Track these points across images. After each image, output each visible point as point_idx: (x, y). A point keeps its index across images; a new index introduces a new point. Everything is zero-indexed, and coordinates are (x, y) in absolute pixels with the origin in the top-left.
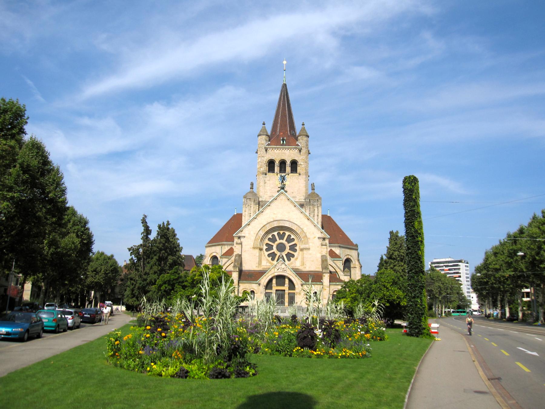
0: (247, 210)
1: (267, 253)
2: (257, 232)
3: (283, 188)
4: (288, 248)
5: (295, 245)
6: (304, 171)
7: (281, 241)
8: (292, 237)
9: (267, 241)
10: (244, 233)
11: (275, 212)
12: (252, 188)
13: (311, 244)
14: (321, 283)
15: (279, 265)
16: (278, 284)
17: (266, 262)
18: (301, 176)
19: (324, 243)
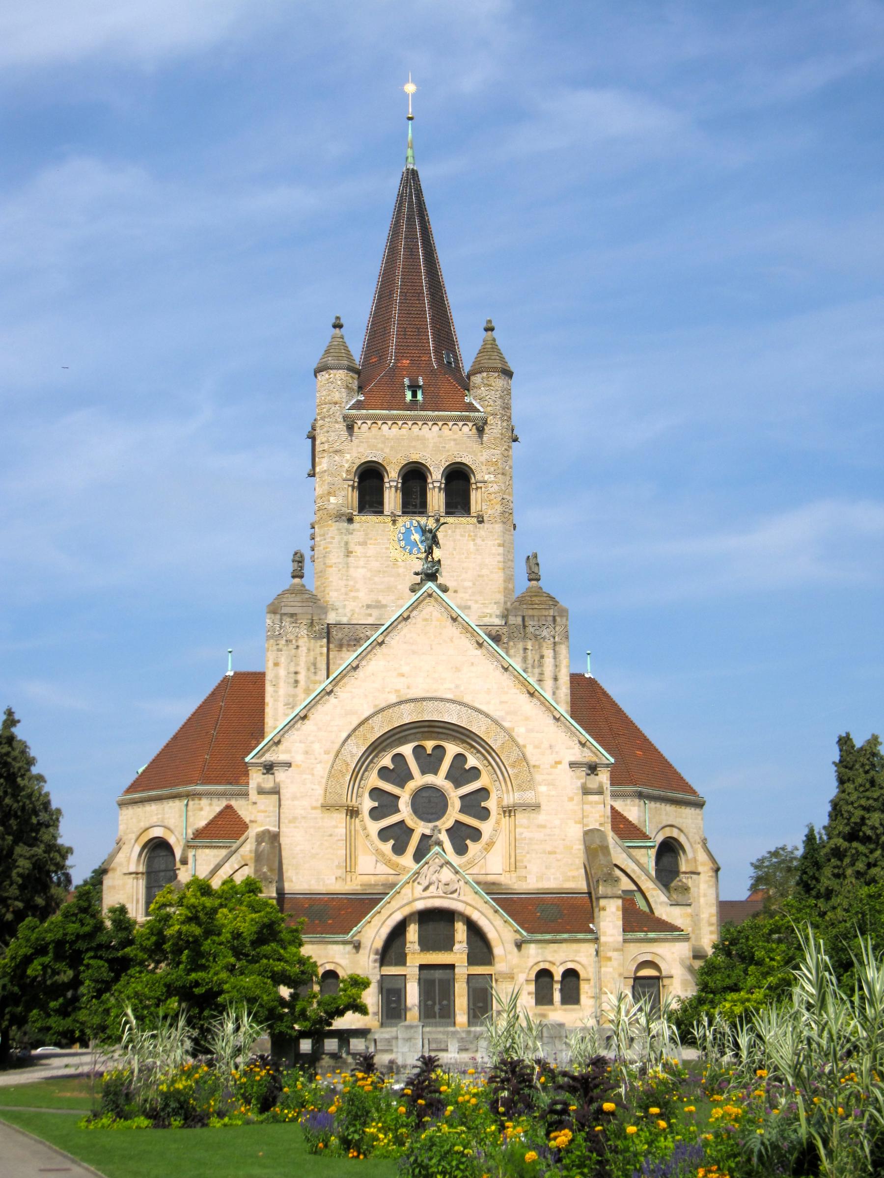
0: (283, 660)
1: (375, 827)
2: (337, 746)
3: (431, 576)
4: (458, 804)
5: (484, 792)
6: (499, 508)
7: (430, 779)
8: (472, 761)
9: (373, 780)
10: (288, 751)
11: (405, 669)
12: (298, 574)
13: (542, 789)
14: (589, 936)
15: (432, 869)
16: (426, 945)
17: (374, 858)
18: (486, 525)
19: (593, 782)
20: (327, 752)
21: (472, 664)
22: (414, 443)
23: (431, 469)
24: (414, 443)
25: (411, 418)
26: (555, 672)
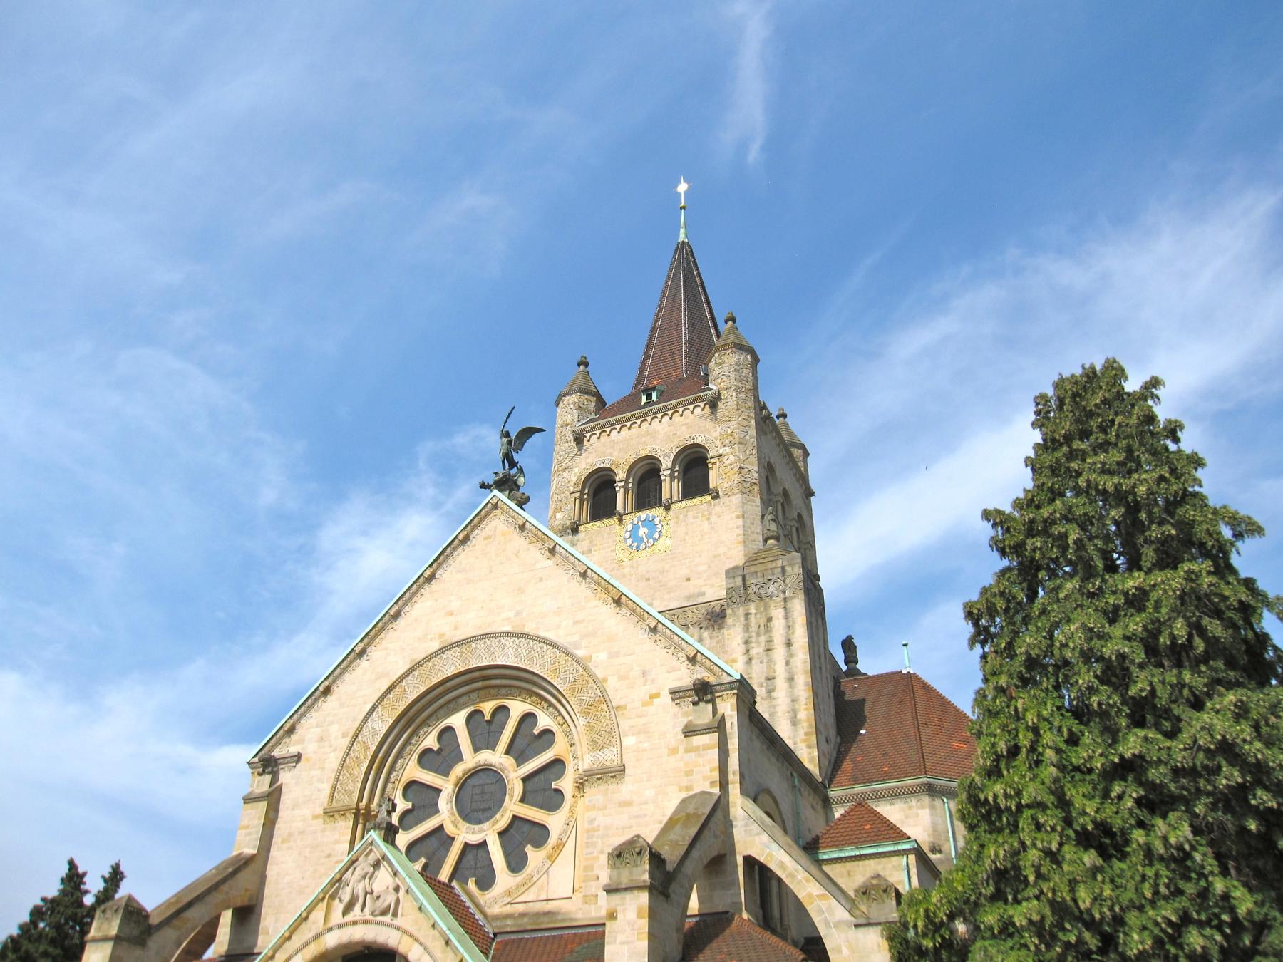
6: (737, 478)
7: (486, 757)
8: (544, 721)
9: (412, 770)
13: (628, 741)
18: (721, 500)
20: (344, 736)
21: (541, 580)
22: (643, 439)
23: (661, 459)
24: (643, 439)
25: (639, 416)
26: (787, 633)
